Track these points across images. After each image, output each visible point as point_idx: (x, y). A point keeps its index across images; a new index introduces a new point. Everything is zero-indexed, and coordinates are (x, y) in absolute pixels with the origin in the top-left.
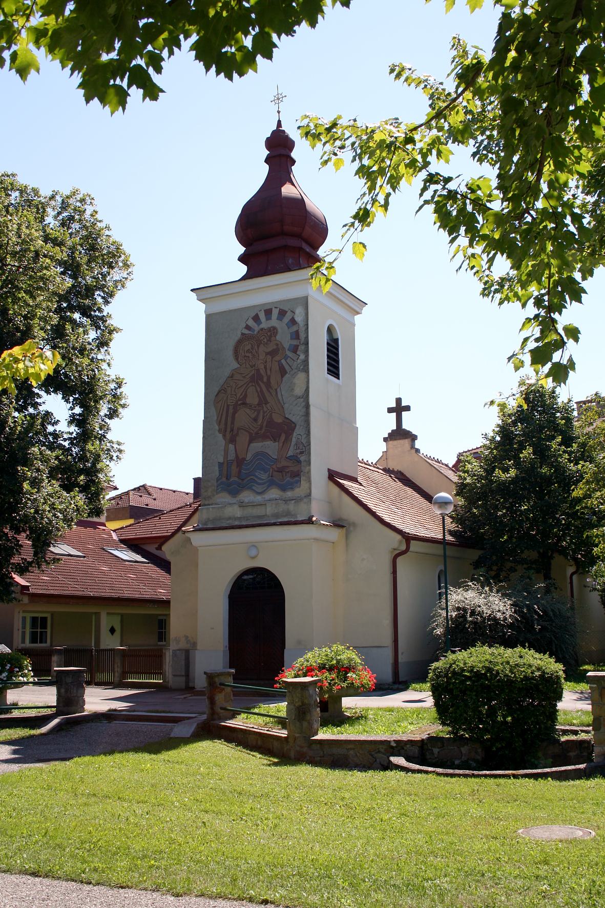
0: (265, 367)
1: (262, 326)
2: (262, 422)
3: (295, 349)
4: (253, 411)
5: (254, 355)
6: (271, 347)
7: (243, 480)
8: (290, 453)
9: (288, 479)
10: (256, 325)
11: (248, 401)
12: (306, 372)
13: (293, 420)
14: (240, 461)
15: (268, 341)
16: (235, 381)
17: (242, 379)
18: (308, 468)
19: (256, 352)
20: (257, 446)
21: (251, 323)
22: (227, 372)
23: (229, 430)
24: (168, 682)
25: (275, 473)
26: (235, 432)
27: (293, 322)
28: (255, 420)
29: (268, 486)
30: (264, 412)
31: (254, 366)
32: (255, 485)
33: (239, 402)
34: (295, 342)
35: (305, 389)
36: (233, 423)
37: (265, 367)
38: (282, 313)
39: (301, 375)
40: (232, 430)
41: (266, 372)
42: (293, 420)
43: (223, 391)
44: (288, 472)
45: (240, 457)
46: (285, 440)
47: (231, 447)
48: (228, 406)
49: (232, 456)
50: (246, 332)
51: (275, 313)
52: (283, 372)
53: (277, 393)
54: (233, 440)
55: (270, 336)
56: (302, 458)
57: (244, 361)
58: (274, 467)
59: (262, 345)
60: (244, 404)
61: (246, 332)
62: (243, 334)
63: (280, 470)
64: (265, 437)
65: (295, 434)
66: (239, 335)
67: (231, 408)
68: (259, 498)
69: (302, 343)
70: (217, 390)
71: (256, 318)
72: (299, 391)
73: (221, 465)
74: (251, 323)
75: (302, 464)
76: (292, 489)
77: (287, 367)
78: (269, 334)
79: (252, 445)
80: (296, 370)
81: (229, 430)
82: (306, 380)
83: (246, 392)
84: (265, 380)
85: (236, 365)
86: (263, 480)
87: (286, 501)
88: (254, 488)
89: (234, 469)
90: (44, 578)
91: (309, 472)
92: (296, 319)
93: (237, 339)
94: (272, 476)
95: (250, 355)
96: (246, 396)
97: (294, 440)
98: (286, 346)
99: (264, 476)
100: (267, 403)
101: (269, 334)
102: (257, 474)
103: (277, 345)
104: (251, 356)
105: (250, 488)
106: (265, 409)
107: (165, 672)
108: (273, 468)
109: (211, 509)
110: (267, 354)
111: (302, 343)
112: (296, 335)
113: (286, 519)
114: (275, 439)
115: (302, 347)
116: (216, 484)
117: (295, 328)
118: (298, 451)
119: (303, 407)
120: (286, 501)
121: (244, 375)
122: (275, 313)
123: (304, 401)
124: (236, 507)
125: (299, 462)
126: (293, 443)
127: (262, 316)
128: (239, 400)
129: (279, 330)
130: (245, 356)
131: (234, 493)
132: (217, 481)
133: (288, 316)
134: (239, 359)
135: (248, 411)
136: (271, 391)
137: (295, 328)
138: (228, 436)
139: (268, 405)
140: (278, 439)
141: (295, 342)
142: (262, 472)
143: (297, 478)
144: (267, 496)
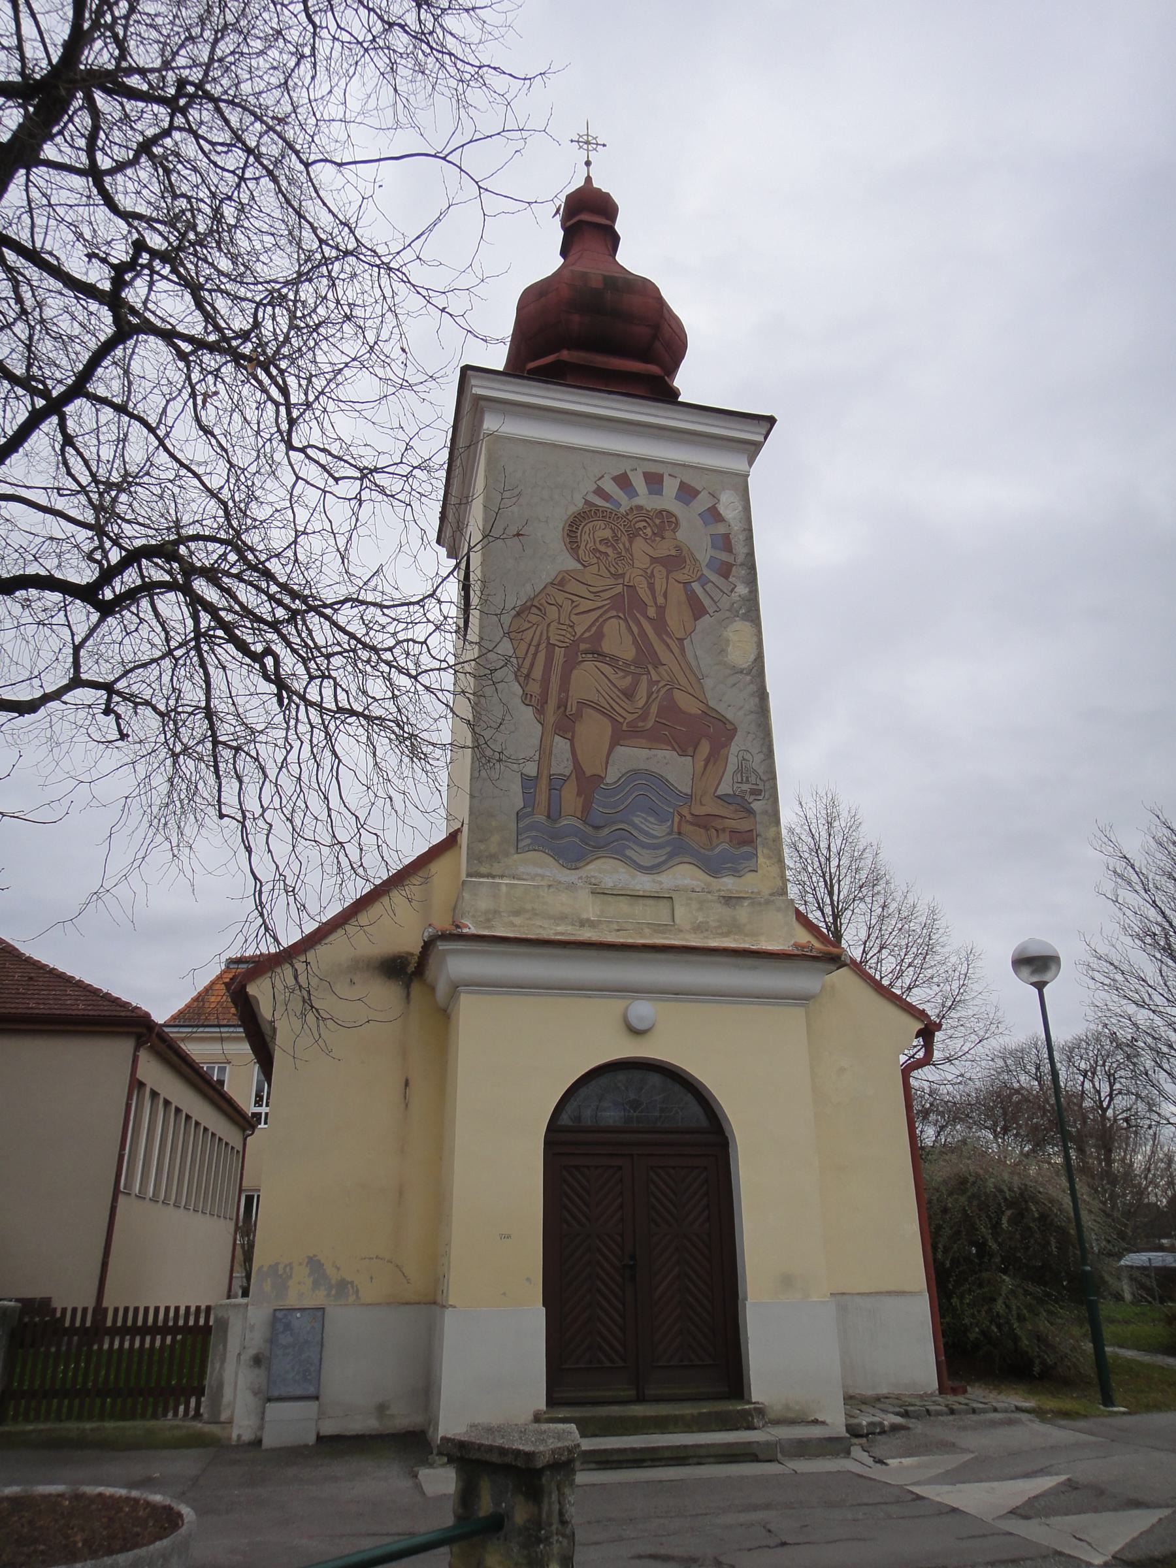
0: (651, 586)
1: (638, 501)
3: (725, 571)
4: (621, 674)
6: (664, 549)
7: (597, 828)
8: (725, 788)
9: (725, 846)
11: (606, 647)
12: (752, 621)
14: (588, 784)
17: (591, 596)
19: (627, 550)
20: (632, 756)
21: (609, 486)
22: (547, 573)
24: (230, 1422)
25: (688, 828)
29: (671, 856)
30: (652, 683)
32: (635, 847)
33: (583, 646)
34: (724, 556)
35: (752, 657)
37: (651, 586)
40: (562, 705)
41: (654, 598)
42: (729, 716)
44: (724, 830)
45: (589, 773)
47: (561, 745)
48: (551, 647)
49: (561, 764)
50: (599, 502)
51: (670, 487)
52: (698, 610)
53: (683, 650)
54: (566, 725)
56: (756, 806)
57: (595, 561)
58: (685, 812)
60: (598, 654)
61: (599, 502)
62: (587, 502)
63: (704, 822)
64: (654, 738)
65: (734, 748)
66: (580, 504)
67: (559, 653)
68: (644, 883)
72: (739, 656)
73: (529, 783)
74: (609, 486)
75: (758, 818)
76: (736, 873)
77: (706, 602)
78: (657, 521)
79: (619, 749)
80: (728, 614)
84: (652, 612)
85: (572, 564)
86: (656, 837)
87: (729, 900)
88: (628, 852)
89: (570, 797)
93: (573, 510)
94: (679, 833)
95: (610, 551)
96: (599, 635)
97: (733, 760)
99: (659, 830)
100: (658, 664)
101: (657, 521)
102: (636, 820)
103: (678, 548)
107: (221, 1385)
108: (680, 814)
109: (504, 889)
112: (725, 542)
114: (685, 747)
115: (739, 572)
116: (513, 826)
118: (745, 787)
119: (752, 695)
122: (670, 487)
123: (752, 682)
125: (751, 812)
126: (731, 767)
129: (683, 523)
130: (596, 550)
133: (702, 503)
134: (581, 552)
137: (721, 529)
138: (551, 717)
140: (690, 751)
141: (724, 556)
142: (651, 819)
143: (746, 849)
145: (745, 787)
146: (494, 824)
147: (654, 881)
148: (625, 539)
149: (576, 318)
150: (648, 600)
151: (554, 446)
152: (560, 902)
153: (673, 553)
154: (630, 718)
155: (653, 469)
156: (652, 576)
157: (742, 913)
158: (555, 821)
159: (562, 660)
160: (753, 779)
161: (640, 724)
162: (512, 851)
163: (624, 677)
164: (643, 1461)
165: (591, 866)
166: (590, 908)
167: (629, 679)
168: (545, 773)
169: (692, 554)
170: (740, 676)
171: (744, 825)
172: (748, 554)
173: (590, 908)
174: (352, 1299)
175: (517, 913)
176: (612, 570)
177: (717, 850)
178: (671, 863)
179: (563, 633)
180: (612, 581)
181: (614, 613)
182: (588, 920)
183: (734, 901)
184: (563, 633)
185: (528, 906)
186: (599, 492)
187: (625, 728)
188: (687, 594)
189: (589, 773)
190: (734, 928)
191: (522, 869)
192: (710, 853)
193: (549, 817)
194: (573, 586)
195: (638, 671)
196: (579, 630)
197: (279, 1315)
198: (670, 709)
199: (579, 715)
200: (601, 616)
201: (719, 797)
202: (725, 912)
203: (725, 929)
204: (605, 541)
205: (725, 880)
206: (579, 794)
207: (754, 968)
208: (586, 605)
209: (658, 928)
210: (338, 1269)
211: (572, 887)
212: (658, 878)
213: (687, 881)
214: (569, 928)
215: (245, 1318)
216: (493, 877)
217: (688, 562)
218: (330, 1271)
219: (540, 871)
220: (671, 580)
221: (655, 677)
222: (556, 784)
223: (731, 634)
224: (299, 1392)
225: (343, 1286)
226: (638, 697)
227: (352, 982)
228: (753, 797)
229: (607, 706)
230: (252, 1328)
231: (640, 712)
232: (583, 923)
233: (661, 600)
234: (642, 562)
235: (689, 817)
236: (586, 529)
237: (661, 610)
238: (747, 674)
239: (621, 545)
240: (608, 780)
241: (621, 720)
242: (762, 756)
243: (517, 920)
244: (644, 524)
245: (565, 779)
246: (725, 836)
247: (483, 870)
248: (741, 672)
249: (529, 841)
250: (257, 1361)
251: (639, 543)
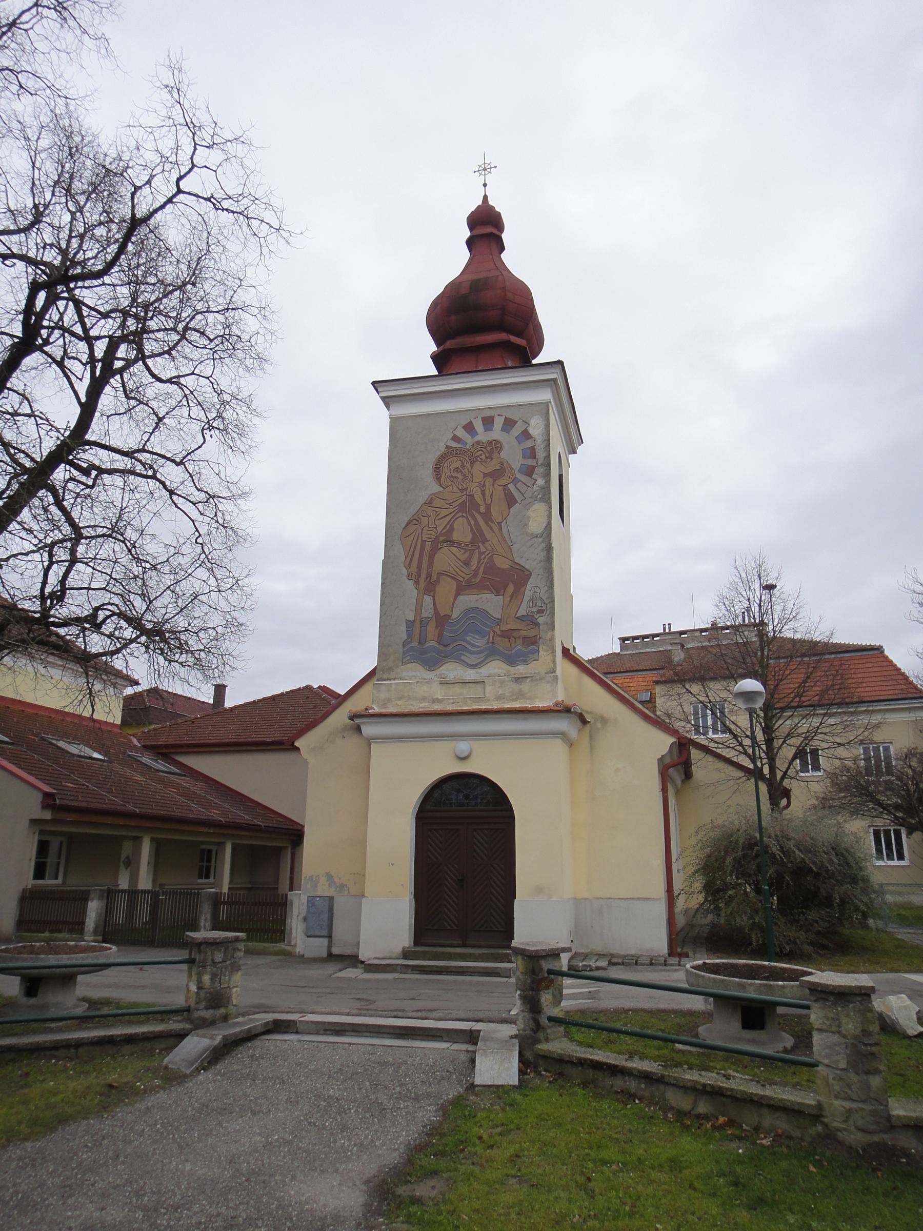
1: (478, 438)
2: (478, 568)
3: (529, 472)
4: (463, 551)
6: (493, 466)
7: (445, 646)
8: (522, 612)
9: (519, 647)
11: (455, 537)
12: (546, 502)
14: (441, 620)
15: (487, 458)
16: (437, 510)
18: (550, 633)
19: (469, 472)
20: (468, 600)
21: (461, 433)
22: (423, 496)
23: (423, 576)
24: (295, 946)
25: (497, 639)
26: (434, 577)
28: (467, 563)
29: (487, 657)
30: (481, 554)
31: (466, 489)
32: (467, 654)
33: (441, 539)
34: (530, 462)
35: (544, 525)
38: (509, 424)
40: (429, 576)
41: (485, 500)
42: (527, 567)
43: (415, 522)
44: (519, 637)
45: (442, 614)
47: (428, 599)
48: (423, 542)
49: (427, 612)
50: (454, 445)
51: (498, 423)
52: (511, 501)
53: (501, 529)
54: (430, 588)
55: (491, 452)
56: (541, 620)
57: (450, 483)
58: (497, 629)
60: (450, 541)
61: (454, 445)
62: (447, 447)
63: (507, 635)
64: (480, 587)
65: (529, 586)
66: (442, 449)
67: (428, 545)
68: (471, 675)
70: (406, 520)
71: (469, 428)
72: (536, 525)
73: (410, 624)
74: (461, 433)
75: (541, 627)
76: (525, 662)
77: (517, 495)
79: (460, 597)
80: (531, 500)
81: (423, 576)
82: (547, 513)
84: (482, 509)
85: (436, 488)
86: (478, 647)
87: (518, 680)
88: (463, 658)
89: (431, 630)
92: (530, 432)
93: (438, 453)
94: (493, 643)
95: (459, 475)
96: (452, 530)
98: (516, 466)
99: (481, 642)
100: (485, 540)
101: (489, 449)
102: (468, 638)
103: (501, 464)
106: (483, 549)
107: (291, 929)
108: (494, 632)
109: (393, 686)
110: (486, 475)
112: (531, 453)
113: (517, 705)
115: (540, 470)
116: (401, 650)
117: (529, 444)
118: (534, 609)
119: (543, 550)
120: (518, 680)
122: (498, 423)
123: (543, 542)
125: (537, 625)
126: (526, 598)
127: (479, 426)
128: (441, 534)
129: (505, 446)
130: (451, 476)
131: (431, 664)
133: (517, 430)
134: (442, 480)
135: (455, 550)
136: (492, 525)
137: (529, 444)
138: (422, 584)
139: (487, 544)
140: (502, 592)
141: (530, 462)
142: (477, 637)
143: (533, 647)
144: (484, 671)
145: (534, 609)
146: (391, 650)
147: (477, 673)
148: (468, 465)
150: (480, 501)
151: (428, 415)
152: (423, 690)
153: (498, 467)
154: (467, 577)
155: (488, 414)
156: (484, 485)
157: (525, 687)
158: (423, 644)
159: (430, 549)
160: (539, 604)
161: (473, 580)
162: (400, 664)
163: (465, 553)
164: (443, 972)
165: (442, 668)
166: (438, 692)
167: (467, 554)
168: (419, 618)
169: (509, 465)
170: (535, 539)
171: (531, 633)
172: (545, 457)
173: (438, 692)
174: (346, 893)
175: (400, 699)
176: (460, 488)
177: (514, 651)
178: (487, 661)
179: (430, 532)
180: (460, 494)
181: (461, 514)
182: (437, 699)
183: (521, 680)
184: (430, 532)
185: (406, 694)
186: (455, 438)
187: (464, 584)
188: (505, 492)
189: (442, 614)
190: (520, 695)
191: (405, 674)
192: (510, 653)
193: (419, 643)
194: (437, 502)
195: (474, 547)
196: (439, 529)
197: (310, 899)
198: (491, 568)
199: (438, 581)
200: (452, 518)
201: (517, 618)
202: (515, 687)
203: (515, 697)
204: (456, 470)
205: (519, 667)
206: (436, 627)
207: (526, 719)
208: (445, 512)
209: (478, 700)
211: (429, 682)
212: (479, 670)
213: (496, 671)
214: (427, 704)
215: (300, 899)
216: (390, 680)
217: (507, 471)
218: (336, 880)
219: (414, 674)
220: (496, 485)
221: (483, 549)
222: (424, 623)
223: (532, 514)
224: (319, 934)
225: (342, 887)
226: (472, 564)
227: (344, 737)
228: (538, 615)
229: (454, 573)
230: (303, 904)
231: (473, 573)
232: (434, 701)
233: (488, 500)
234: (478, 477)
235: (499, 632)
236: (446, 465)
237: (488, 507)
238: (541, 536)
239: (466, 470)
240: (453, 617)
241: (462, 580)
242: (546, 588)
243: (400, 703)
244: (481, 452)
245: (429, 620)
246: (520, 641)
247: (385, 676)
248: (537, 537)
249: (409, 657)
250: (305, 919)
251: (477, 465)
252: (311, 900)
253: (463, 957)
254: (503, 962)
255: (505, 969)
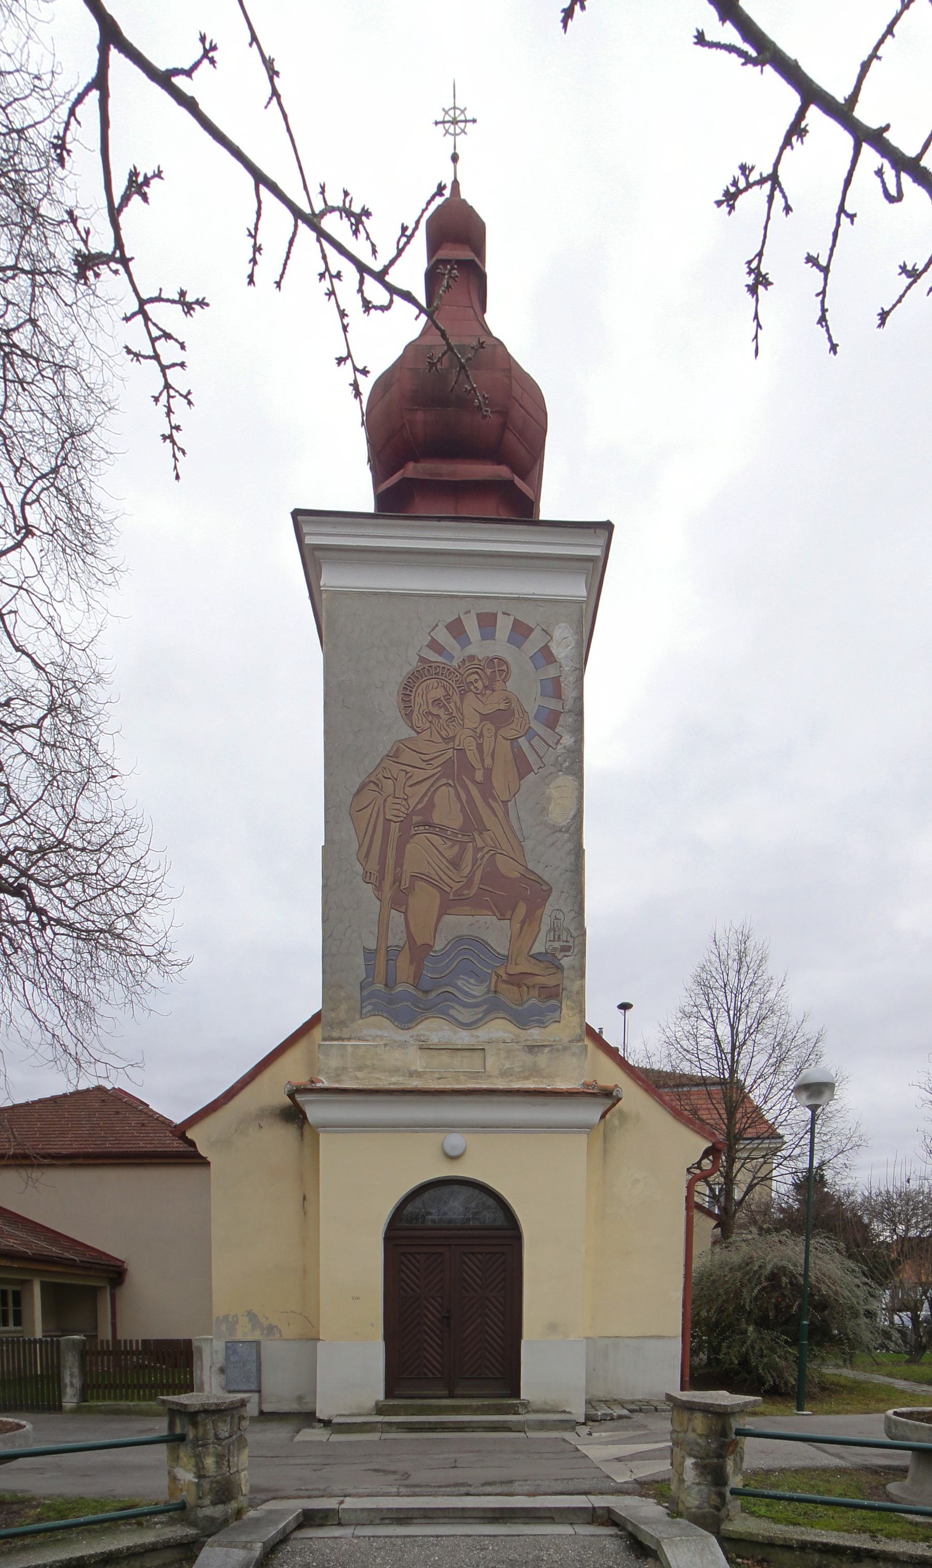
0: (480, 747)
1: (471, 650)
2: (472, 873)
3: (552, 720)
4: (449, 843)
5: (451, 717)
6: (493, 703)
7: (426, 992)
9: (534, 1001)
10: (458, 647)
11: (437, 817)
12: (575, 774)
13: (546, 878)
15: (485, 687)
16: (409, 769)
17: (423, 765)
18: (578, 983)
19: (458, 709)
21: (443, 637)
22: (385, 743)
23: (389, 878)
25: (503, 987)
26: (405, 884)
27: (546, 655)
28: (455, 863)
29: (487, 1012)
30: (477, 850)
31: (453, 739)
32: (457, 1006)
33: (416, 819)
34: (553, 704)
35: (573, 813)
36: (399, 863)
37: (480, 747)
38: (521, 631)
39: (565, 781)
40: (397, 880)
41: (483, 760)
43: (372, 786)
44: (534, 986)
45: (420, 942)
46: (526, 916)
47: (396, 917)
49: (397, 938)
50: (433, 656)
51: (504, 626)
52: (523, 767)
53: (507, 813)
55: (492, 679)
56: (565, 962)
58: (501, 972)
59: (470, 696)
60: (429, 825)
61: (433, 656)
62: (422, 660)
63: (517, 980)
64: (477, 904)
65: (548, 908)
66: (414, 661)
68: (464, 1038)
69: (567, 708)
70: (358, 781)
71: (456, 628)
72: (558, 815)
73: (370, 955)
74: (443, 637)
75: (566, 973)
76: (542, 1024)
77: (532, 758)
78: (489, 671)
79: (446, 918)
80: (553, 769)
81: (389, 878)
82: (576, 793)
83: (432, 797)
84: (479, 776)
85: (407, 732)
86: (474, 997)
87: (532, 1049)
88: (451, 1012)
89: (404, 968)
90: (468, 1332)
91: (581, 992)
92: (554, 651)
93: (408, 669)
94: (496, 992)
95: (441, 712)
96: (431, 805)
97: (546, 920)
98: (531, 708)
99: (478, 990)
100: (482, 829)
101: (489, 671)
102: (459, 983)
103: (508, 700)
104: (444, 717)
105: (444, 1014)
106: (480, 844)
108: (498, 976)
109: (350, 1049)
110: (484, 717)
111: (567, 708)
112: (554, 688)
113: (530, 1085)
114: (503, 911)
115: (566, 720)
116: (358, 995)
117: (551, 672)
118: (557, 945)
119: (569, 853)
120: (532, 1049)
121: (426, 757)
122: (504, 626)
123: (569, 840)
124: (413, 1051)
125: (560, 968)
126: (544, 928)
127: (472, 628)
128: (414, 812)
129: (514, 668)
131: (405, 1020)
132: (362, 989)
134: (415, 717)
135: (436, 840)
136: (494, 805)
137: (551, 672)
138: (388, 893)
139: (486, 835)
140: (508, 915)
141: (553, 704)
142: (472, 981)
144: (483, 1034)
145: (557, 945)
146: (343, 994)
147: (472, 1036)
148: (456, 698)
149: (420, 416)
150: (476, 764)
152: (394, 1058)
153: (502, 707)
154: (456, 886)
155: (487, 608)
156: (481, 735)
157: (542, 1059)
158: (392, 988)
159: (397, 835)
160: (564, 937)
161: (465, 892)
162: (357, 1016)
163: (452, 846)
164: (437, 1428)
165: (419, 1027)
166: (418, 1062)
167: (456, 848)
168: (383, 945)
169: (521, 705)
170: (558, 835)
171: (551, 981)
172: (576, 698)
173: (418, 1062)
174: (277, 1336)
175: (360, 1069)
176: (444, 734)
177: (526, 1006)
178: (487, 1019)
179: (398, 807)
180: (444, 746)
181: (444, 781)
182: (416, 1071)
183: (536, 1049)
184: (398, 807)
185: (369, 1063)
186: (434, 645)
187: (451, 897)
188: (513, 752)
189: (419, 942)
190: (535, 1071)
191: (365, 1032)
192: (520, 1008)
193: (386, 985)
194: (408, 757)
195: (466, 839)
196: (412, 802)
197: (228, 1344)
198: (493, 876)
199: (411, 888)
200: (432, 785)
201: (532, 956)
202: (528, 1058)
203: (527, 1074)
204: (437, 702)
205: (532, 1031)
206: (411, 962)
208: (420, 775)
209: (474, 1075)
210: (267, 1318)
211: (403, 1045)
212: (474, 1032)
213: (500, 1034)
214: (401, 1079)
216: (342, 1039)
217: (517, 715)
218: (262, 1320)
219: (379, 1033)
220: (499, 737)
221: (480, 844)
222: (392, 954)
223: (553, 792)
224: (245, 1388)
225: (271, 1329)
226: (463, 866)
228: (562, 954)
229: (437, 878)
231: (465, 880)
232: (412, 1074)
233: (488, 761)
234: (472, 720)
235: (504, 977)
236: (420, 691)
237: (488, 772)
238: (567, 832)
239: (452, 705)
240: (437, 948)
241: (448, 889)
242: (573, 914)
243: (360, 1074)
244: (476, 677)
245: (399, 950)
246: (535, 992)
247: (335, 1034)
248: (560, 831)
249: (370, 1007)
251: (470, 697)
252: (231, 1347)
253: (456, 1410)
254: (508, 1414)
255: (519, 1422)
